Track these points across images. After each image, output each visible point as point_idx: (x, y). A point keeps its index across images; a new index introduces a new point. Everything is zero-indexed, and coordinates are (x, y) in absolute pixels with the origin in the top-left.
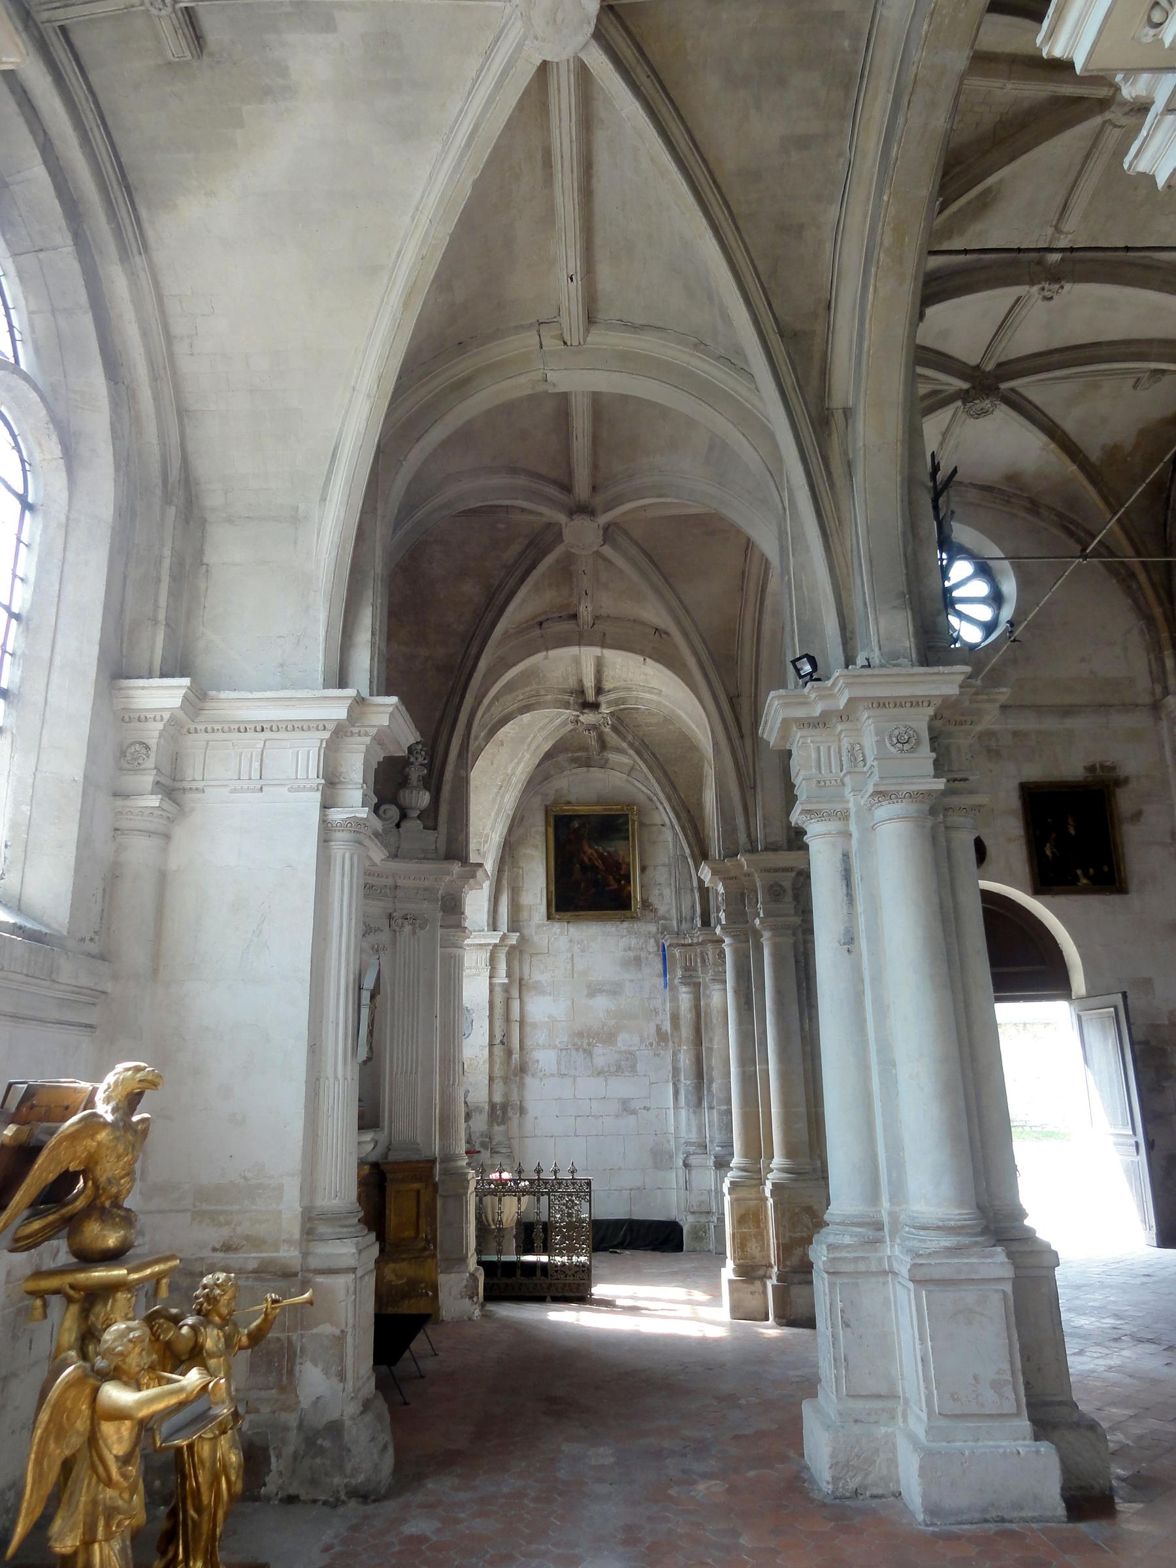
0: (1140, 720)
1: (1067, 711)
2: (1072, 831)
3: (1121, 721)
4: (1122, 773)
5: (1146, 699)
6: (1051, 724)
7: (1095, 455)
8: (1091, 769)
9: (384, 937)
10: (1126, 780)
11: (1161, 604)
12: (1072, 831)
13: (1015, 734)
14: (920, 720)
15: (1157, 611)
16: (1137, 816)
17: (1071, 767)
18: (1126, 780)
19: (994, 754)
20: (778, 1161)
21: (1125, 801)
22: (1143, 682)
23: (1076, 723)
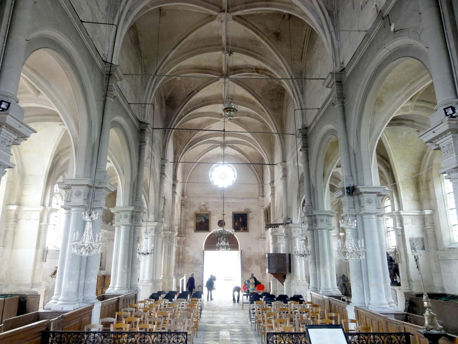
0: (255, 201)
1: (243, 199)
2: (241, 221)
3: (252, 201)
4: (251, 210)
5: (257, 197)
6: (240, 201)
7: (248, 154)
8: (246, 209)
9: (108, 242)
10: (252, 212)
11: (260, 179)
12: (241, 221)
13: (233, 202)
14: (153, 228)
15: (260, 181)
16: (253, 218)
17: (241, 209)
18: (252, 212)
19: (229, 206)
20: (162, 276)
21: (250, 216)
22: (257, 193)
23: (244, 201)
